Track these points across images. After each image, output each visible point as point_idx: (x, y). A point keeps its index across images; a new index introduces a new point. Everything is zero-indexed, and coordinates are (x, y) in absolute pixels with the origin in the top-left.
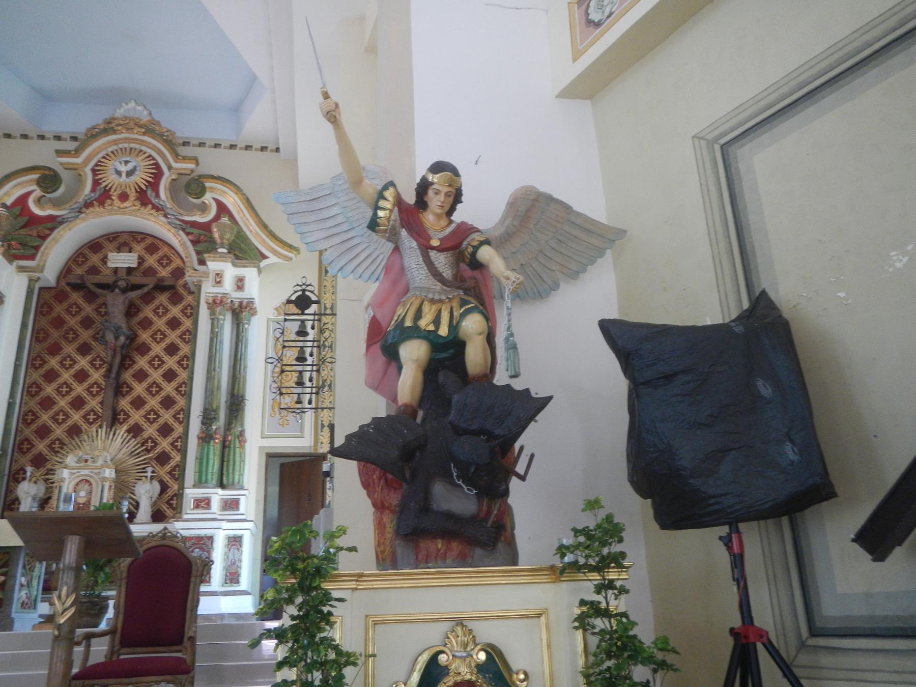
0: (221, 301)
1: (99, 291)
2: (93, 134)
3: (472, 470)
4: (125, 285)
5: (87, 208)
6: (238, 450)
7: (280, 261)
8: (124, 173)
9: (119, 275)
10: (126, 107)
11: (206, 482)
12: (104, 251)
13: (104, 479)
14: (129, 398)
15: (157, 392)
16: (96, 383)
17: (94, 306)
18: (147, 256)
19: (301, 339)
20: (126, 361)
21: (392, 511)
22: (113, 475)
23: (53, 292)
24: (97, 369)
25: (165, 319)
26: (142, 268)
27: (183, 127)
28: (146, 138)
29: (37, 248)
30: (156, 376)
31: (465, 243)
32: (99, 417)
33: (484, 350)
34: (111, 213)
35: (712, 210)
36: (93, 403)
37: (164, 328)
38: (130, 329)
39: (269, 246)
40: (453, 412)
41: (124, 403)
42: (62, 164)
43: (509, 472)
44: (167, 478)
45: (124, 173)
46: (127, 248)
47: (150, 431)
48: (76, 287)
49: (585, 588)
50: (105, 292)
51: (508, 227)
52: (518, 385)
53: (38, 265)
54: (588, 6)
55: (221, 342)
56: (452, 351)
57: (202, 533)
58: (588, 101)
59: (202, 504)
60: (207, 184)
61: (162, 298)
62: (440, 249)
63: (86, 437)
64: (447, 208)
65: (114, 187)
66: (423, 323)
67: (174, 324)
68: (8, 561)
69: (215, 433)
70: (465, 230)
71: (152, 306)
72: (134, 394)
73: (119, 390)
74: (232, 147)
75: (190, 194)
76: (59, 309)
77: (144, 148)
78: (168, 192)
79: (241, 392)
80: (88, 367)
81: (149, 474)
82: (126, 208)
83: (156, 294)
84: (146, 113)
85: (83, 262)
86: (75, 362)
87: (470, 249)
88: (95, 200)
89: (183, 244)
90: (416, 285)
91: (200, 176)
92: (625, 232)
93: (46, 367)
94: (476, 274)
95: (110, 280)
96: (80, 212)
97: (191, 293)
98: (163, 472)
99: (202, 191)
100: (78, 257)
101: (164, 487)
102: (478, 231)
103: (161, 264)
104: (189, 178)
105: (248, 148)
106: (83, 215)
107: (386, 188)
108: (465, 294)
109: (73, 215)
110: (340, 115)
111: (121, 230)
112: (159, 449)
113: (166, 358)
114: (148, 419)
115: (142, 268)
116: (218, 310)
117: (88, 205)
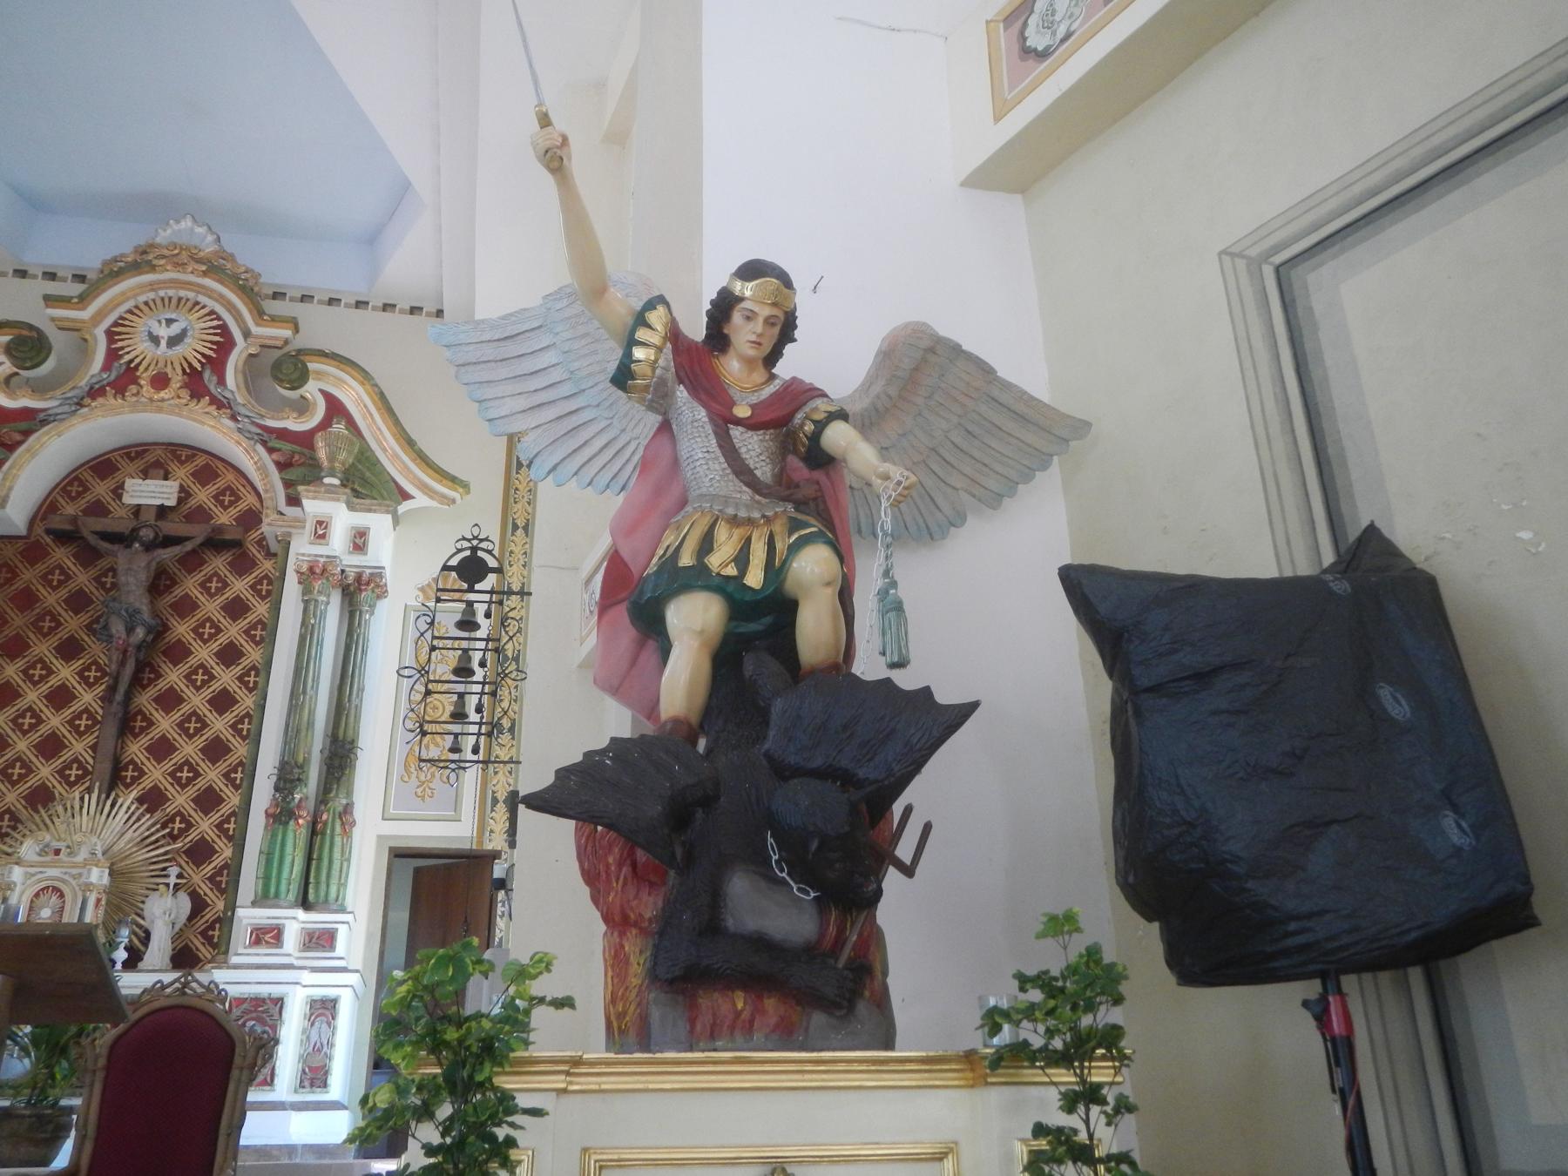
0: (324, 570)
1: (105, 545)
2: (114, 271)
3: (814, 845)
4: (152, 536)
5: (94, 399)
6: (338, 840)
7: (434, 504)
8: (163, 340)
9: (144, 517)
10: (176, 227)
11: (277, 895)
12: (118, 476)
13: (88, 887)
14: (145, 741)
15: (197, 731)
16: (86, 710)
17: (93, 572)
18: (195, 488)
19: (465, 634)
20: (144, 673)
21: (643, 931)
22: (106, 880)
23: (20, 545)
24: (90, 685)
25: (220, 600)
26: (185, 509)
27: (276, 267)
28: (208, 282)
30: (197, 701)
31: (799, 416)
33: (835, 617)
34: (134, 408)
35: (1259, 385)
38: (155, 614)
39: (415, 476)
40: (772, 733)
41: (136, 749)
42: (53, 319)
43: (883, 857)
44: (205, 889)
45: (163, 340)
46: (162, 472)
47: (181, 800)
48: (63, 537)
49: (1044, 1097)
50: (116, 547)
51: (878, 397)
52: (906, 680)
54: (1025, 24)
55: (320, 644)
56: (768, 620)
57: (264, 991)
58: (1019, 197)
59: (267, 937)
61: (218, 563)
62: (751, 425)
63: (60, 809)
64: (767, 348)
66: (714, 561)
67: (236, 609)
69: (299, 806)
70: (799, 394)
71: (199, 577)
72: (155, 733)
73: (129, 724)
74: (360, 304)
75: (280, 381)
77: (202, 299)
80: (73, 681)
81: (172, 880)
82: (163, 400)
83: (208, 555)
84: (210, 238)
85: (79, 494)
86: (50, 672)
87: (809, 427)
89: (262, 469)
90: (704, 490)
91: (299, 352)
92: (1088, 425)
94: (818, 475)
95: (124, 527)
96: (80, 405)
97: (270, 555)
98: (199, 877)
99: (302, 378)
100: (72, 484)
101: (199, 905)
102: (824, 395)
103: (221, 503)
104: (278, 353)
105: (388, 307)
106: (85, 410)
107: (650, 305)
108: (797, 510)
109: (66, 409)
110: (570, 159)
111: (150, 439)
112: (193, 835)
113: (218, 670)
115: (185, 509)
116: (317, 585)
117: (95, 392)
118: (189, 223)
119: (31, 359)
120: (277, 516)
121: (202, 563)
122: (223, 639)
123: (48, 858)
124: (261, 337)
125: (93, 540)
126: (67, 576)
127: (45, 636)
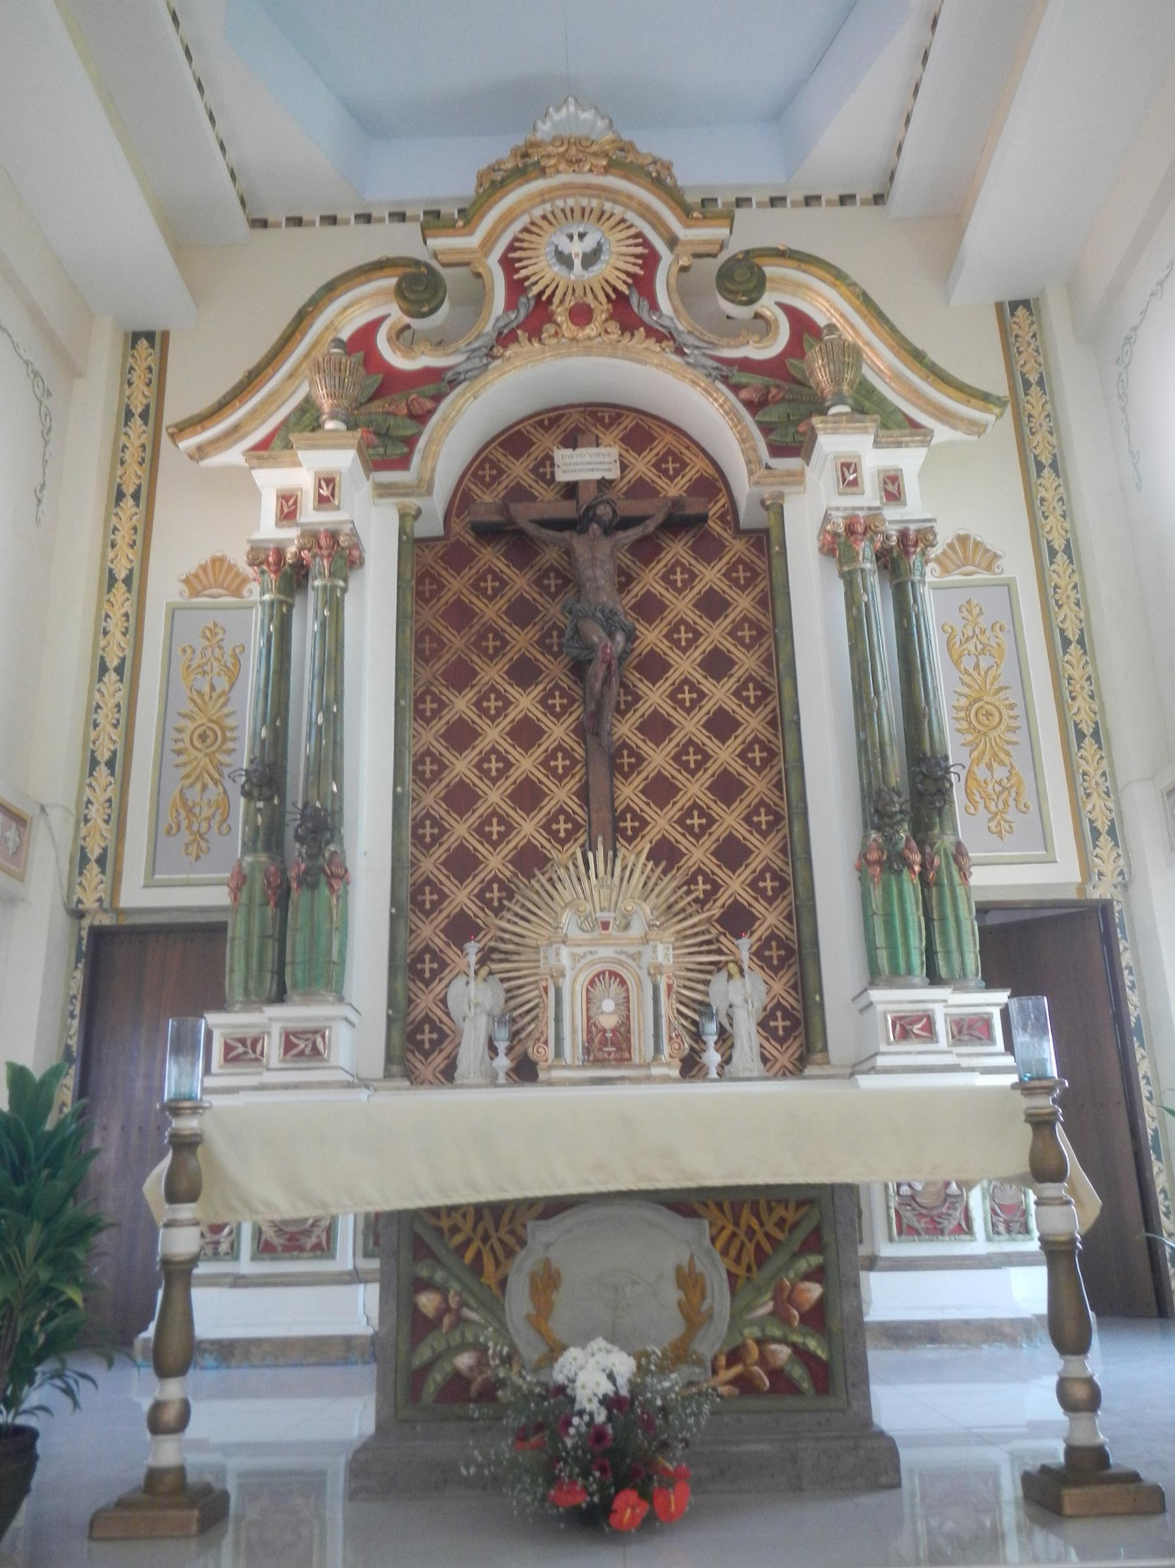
2: (494, 184)
5: (505, 347)
8: (578, 258)
10: (556, 117)
12: (536, 452)
14: (638, 781)
17: (530, 574)
23: (440, 548)
24: (558, 716)
25: (691, 595)
28: (613, 181)
29: (410, 442)
32: (577, 827)
36: (562, 795)
37: (692, 616)
41: (629, 792)
45: (578, 258)
48: (487, 533)
53: (420, 480)
60: (770, 270)
61: (678, 550)
63: (562, 872)
65: (559, 294)
68: (817, 1232)
71: (659, 568)
76: (457, 585)
78: (676, 296)
79: (938, 746)
80: (537, 713)
82: (589, 338)
83: (665, 541)
84: (601, 124)
85: (494, 479)
86: (507, 703)
88: (518, 327)
91: (747, 253)
93: (448, 716)
100: (482, 468)
103: (665, 472)
105: (810, 200)
106: (498, 362)
111: (563, 401)
113: (707, 685)
114: (690, 829)
117: (505, 338)
118: (572, 109)
119: (428, 301)
120: (763, 471)
121: (659, 549)
122: (705, 646)
123: (595, 935)
124: (691, 242)
125: (532, 529)
126: (503, 583)
127: (491, 658)
